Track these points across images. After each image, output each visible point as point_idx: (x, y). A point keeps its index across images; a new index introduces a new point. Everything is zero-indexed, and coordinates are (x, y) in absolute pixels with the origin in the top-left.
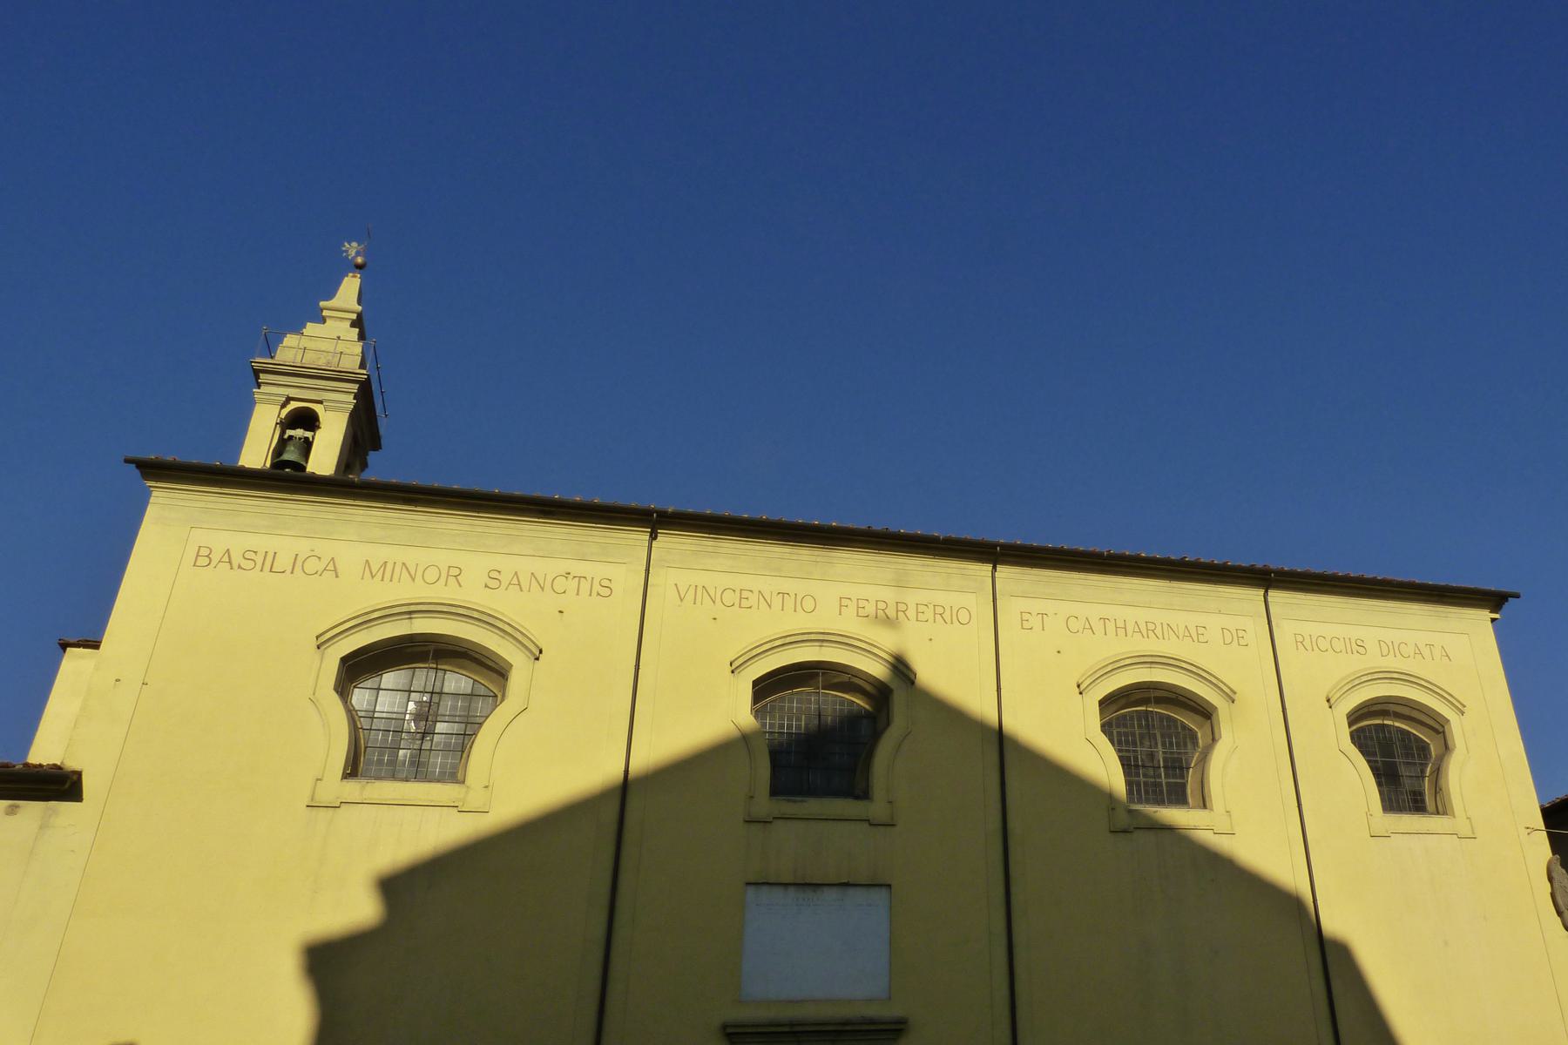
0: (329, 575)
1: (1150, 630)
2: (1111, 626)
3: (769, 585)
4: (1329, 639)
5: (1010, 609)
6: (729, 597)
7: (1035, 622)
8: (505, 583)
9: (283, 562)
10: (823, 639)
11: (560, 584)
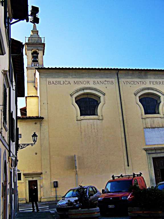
0: (69, 84)
9: (62, 83)
10: (148, 89)
11: (105, 82)
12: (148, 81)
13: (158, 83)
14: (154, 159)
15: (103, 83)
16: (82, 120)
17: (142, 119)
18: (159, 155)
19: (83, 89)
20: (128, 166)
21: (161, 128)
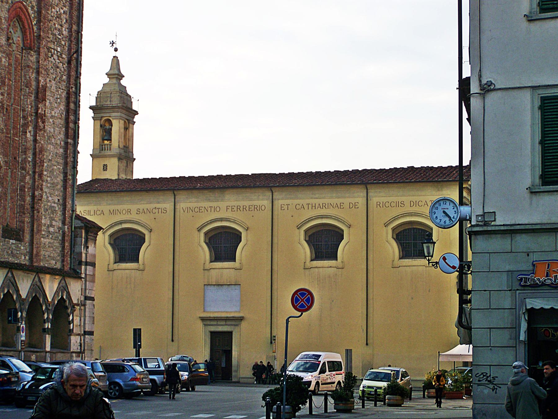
1: (324, 206)
2: (310, 206)
3: (207, 204)
4: (390, 203)
5: (278, 203)
6: (196, 210)
7: (286, 207)
8: (141, 213)
10: (221, 220)
12: (223, 205)
13: (241, 209)
14: (212, 333)
15: (151, 212)
16: (115, 271)
17: (204, 270)
18: (220, 329)
19: (121, 223)
20: (173, 341)
21: (233, 286)
